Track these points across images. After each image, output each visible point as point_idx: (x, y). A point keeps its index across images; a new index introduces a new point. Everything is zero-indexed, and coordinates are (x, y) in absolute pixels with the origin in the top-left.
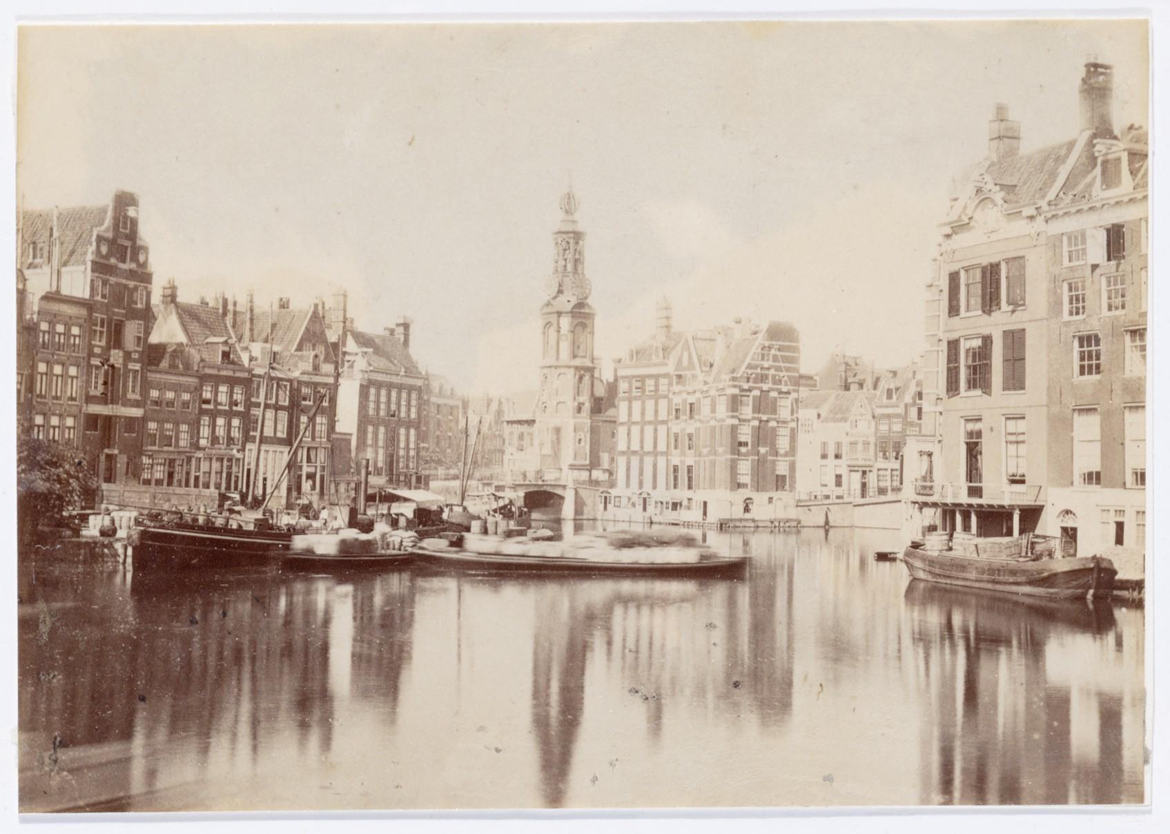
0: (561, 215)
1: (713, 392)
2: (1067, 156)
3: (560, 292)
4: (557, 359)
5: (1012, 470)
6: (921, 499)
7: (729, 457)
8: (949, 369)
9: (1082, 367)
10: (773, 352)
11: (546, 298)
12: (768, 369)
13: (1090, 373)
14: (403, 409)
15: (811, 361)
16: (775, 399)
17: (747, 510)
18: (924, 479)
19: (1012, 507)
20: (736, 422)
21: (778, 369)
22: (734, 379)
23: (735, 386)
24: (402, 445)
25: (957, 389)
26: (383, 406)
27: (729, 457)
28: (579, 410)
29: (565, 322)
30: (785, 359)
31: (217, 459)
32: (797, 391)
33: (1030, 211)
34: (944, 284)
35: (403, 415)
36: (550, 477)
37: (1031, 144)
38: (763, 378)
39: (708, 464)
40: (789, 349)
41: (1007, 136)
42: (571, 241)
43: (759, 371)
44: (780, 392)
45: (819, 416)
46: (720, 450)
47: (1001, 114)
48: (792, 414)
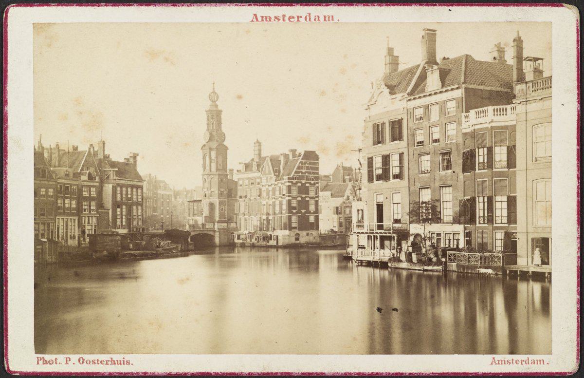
1: (280, 185)
2: (416, 71)
3: (210, 140)
4: (211, 171)
5: (396, 217)
7: (288, 215)
8: (369, 171)
10: (307, 165)
11: (204, 143)
12: (305, 173)
14: (135, 197)
15: (326, 167)
16: (308, 187)
17: (297, 239)
20: (290, 198)
21: (310, 173)
22: (289, 178)
23: (289, 182)
24: (135, 214)
25: (373, 180)
26: (124, 196)
27: (288, 215)
29: (213, 154)
30: (312, 168)
31: (42, 223)
32: (318, 183)
35: (134, 200)
36: (209, 226)
37: (401, 68)
38: (303, 178)
39: (278, 218)
40: (314, 164)
41: (394, 62)
43: (300, 174)
44: (310, 184)
46: (284, 212)
47: (390, 51)
48: (316, 194)
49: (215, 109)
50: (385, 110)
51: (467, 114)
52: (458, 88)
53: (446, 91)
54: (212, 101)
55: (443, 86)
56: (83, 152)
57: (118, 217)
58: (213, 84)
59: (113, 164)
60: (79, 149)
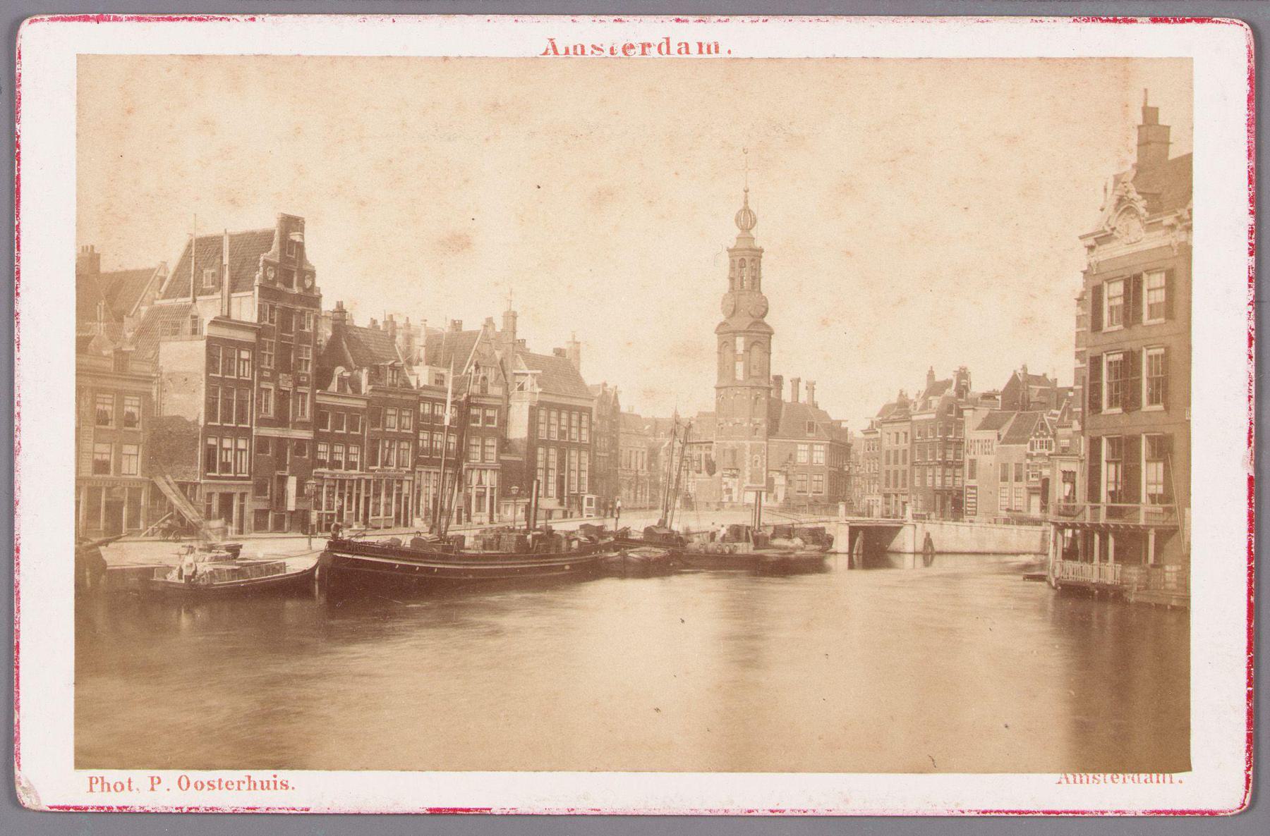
6: (1063, 520)
11: (722, 318)
14: (574, 430)
18: (1067, 498)
19: (1147, 527)
29: (740, 342)
33: (1168, 220)
34: (1089, 297)
42: (747, 262)
45: (999, 436)
47: (1150, 114)
50: (1134, 249)
56: (472, 335)
57: (540, 472)
59: (533, 361)
60: (466, 328)
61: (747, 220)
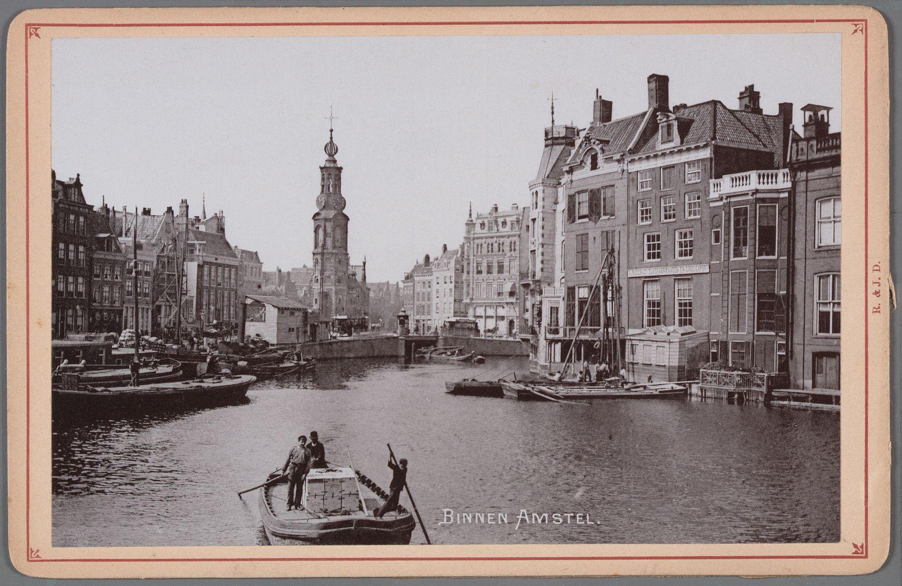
0: (327, 157)
9: (649, 254)
11: (317, 210)
13: (654, 258)
28: (339, 281)
29: (329, 226)
49: (332, 165)
51: (718, 181)
52: (705, 146)
53: (689, 150)
54: (329, 155)
55: (682, 143)
58: (331, 131)
61: (331, 149)
